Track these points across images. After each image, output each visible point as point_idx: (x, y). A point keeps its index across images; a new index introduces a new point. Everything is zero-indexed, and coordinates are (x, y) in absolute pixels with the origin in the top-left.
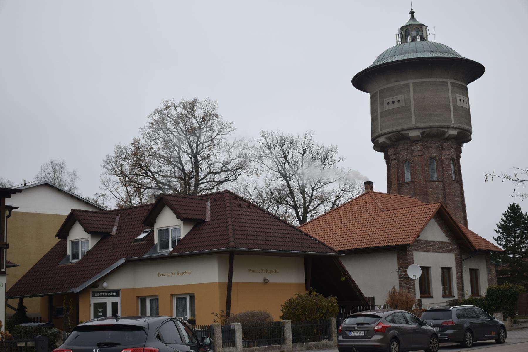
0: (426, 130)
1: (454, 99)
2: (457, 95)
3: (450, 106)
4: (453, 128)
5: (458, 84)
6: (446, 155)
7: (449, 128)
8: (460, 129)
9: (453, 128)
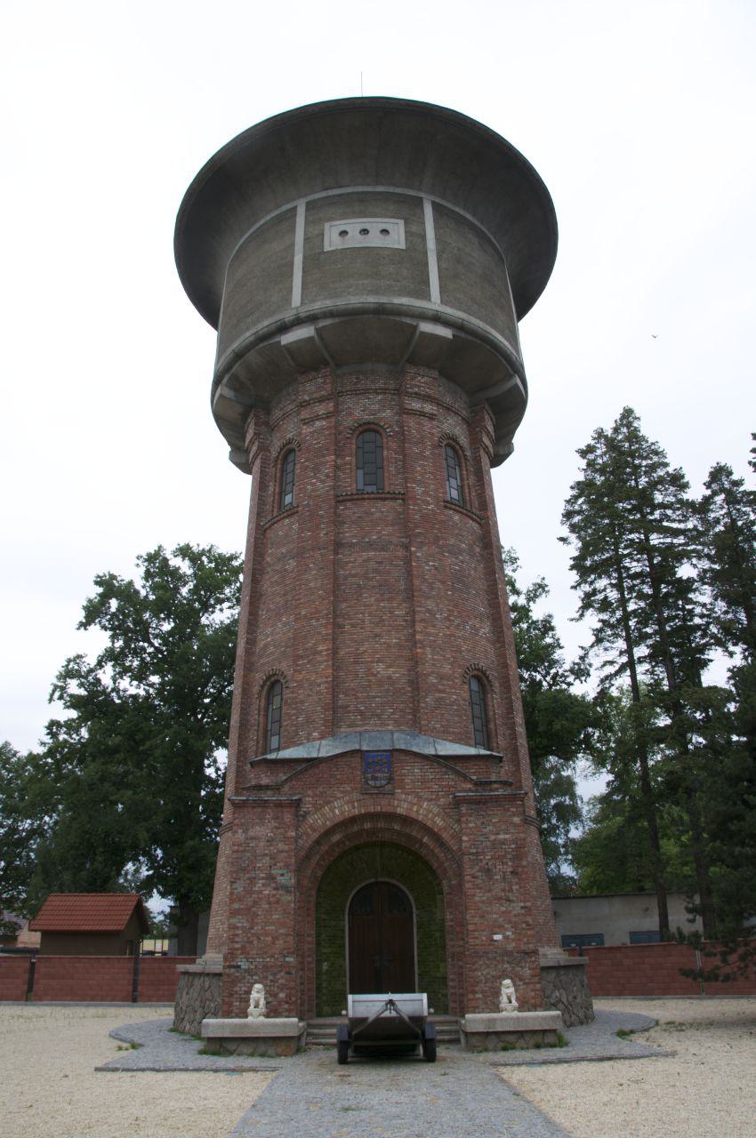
0: (233, 370)
1: (314, 240)
2: (327, 225)
3: (291, 265)
4: (298, 322)
5: (340, 195)
6: (318, 418)
7: (284, 328)
8: (330, 314)
9: (298, 322)
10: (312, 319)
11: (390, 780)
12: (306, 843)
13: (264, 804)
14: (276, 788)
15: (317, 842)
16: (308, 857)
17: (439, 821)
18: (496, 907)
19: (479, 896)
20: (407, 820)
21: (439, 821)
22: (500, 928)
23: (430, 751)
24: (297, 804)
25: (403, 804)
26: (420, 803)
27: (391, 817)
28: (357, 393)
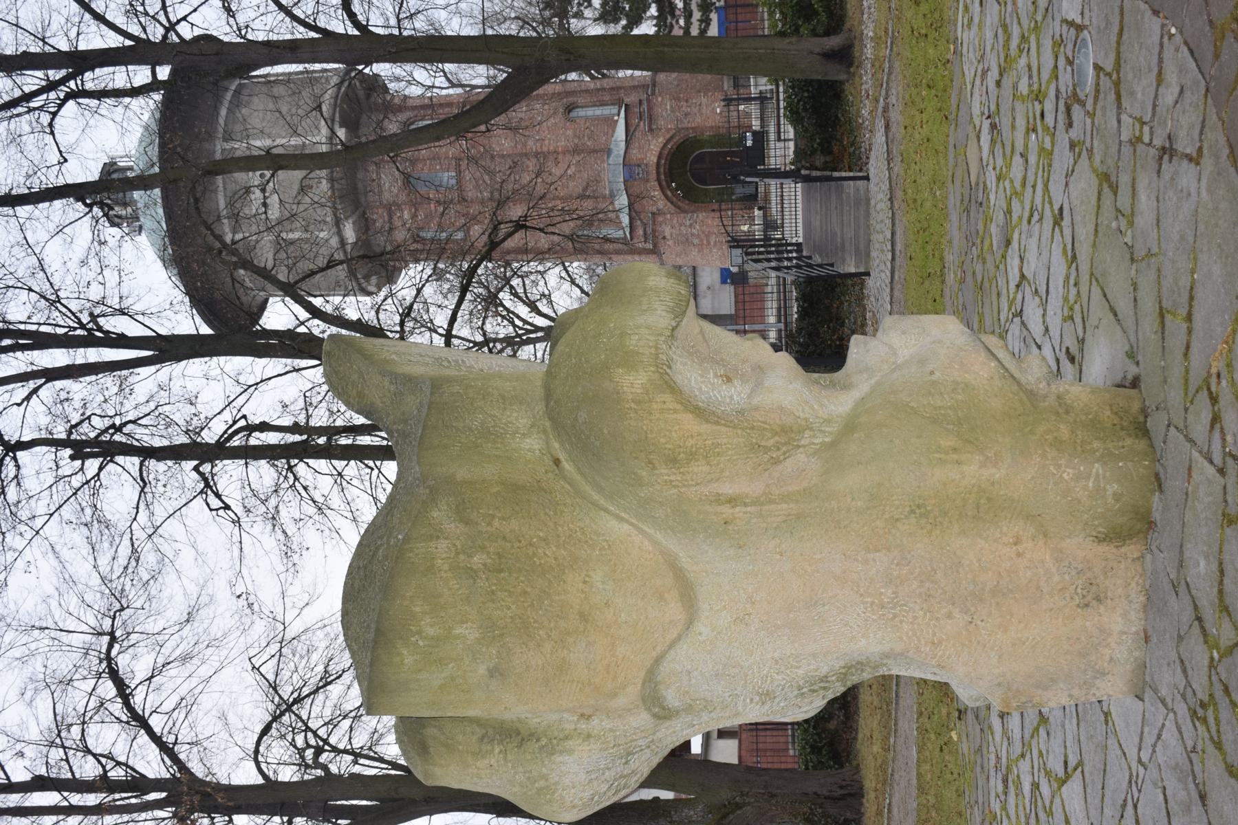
10: (338, 223)
11: (639, 166)
12: (672, 209)
13: (654, 231)
14: (645, 225)
15: (672, 203)
16: (679, 208)
17: (660, 140)
18: (704, 111)
19: (698, 120)
20: (659, 157)
21: (660, 140)
22: (714, 110)
23: (623, 145)
24: (653, 214)
25: (652, 159)
26: (651, 150)
27: (658, 164)
28: (380, 193)
